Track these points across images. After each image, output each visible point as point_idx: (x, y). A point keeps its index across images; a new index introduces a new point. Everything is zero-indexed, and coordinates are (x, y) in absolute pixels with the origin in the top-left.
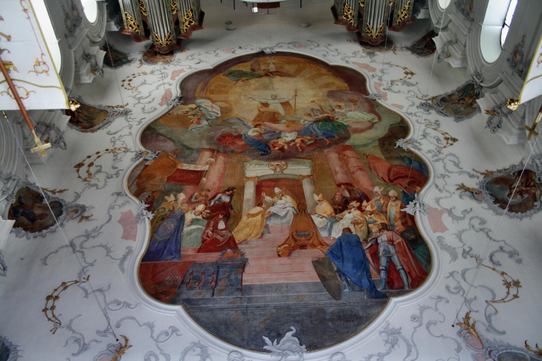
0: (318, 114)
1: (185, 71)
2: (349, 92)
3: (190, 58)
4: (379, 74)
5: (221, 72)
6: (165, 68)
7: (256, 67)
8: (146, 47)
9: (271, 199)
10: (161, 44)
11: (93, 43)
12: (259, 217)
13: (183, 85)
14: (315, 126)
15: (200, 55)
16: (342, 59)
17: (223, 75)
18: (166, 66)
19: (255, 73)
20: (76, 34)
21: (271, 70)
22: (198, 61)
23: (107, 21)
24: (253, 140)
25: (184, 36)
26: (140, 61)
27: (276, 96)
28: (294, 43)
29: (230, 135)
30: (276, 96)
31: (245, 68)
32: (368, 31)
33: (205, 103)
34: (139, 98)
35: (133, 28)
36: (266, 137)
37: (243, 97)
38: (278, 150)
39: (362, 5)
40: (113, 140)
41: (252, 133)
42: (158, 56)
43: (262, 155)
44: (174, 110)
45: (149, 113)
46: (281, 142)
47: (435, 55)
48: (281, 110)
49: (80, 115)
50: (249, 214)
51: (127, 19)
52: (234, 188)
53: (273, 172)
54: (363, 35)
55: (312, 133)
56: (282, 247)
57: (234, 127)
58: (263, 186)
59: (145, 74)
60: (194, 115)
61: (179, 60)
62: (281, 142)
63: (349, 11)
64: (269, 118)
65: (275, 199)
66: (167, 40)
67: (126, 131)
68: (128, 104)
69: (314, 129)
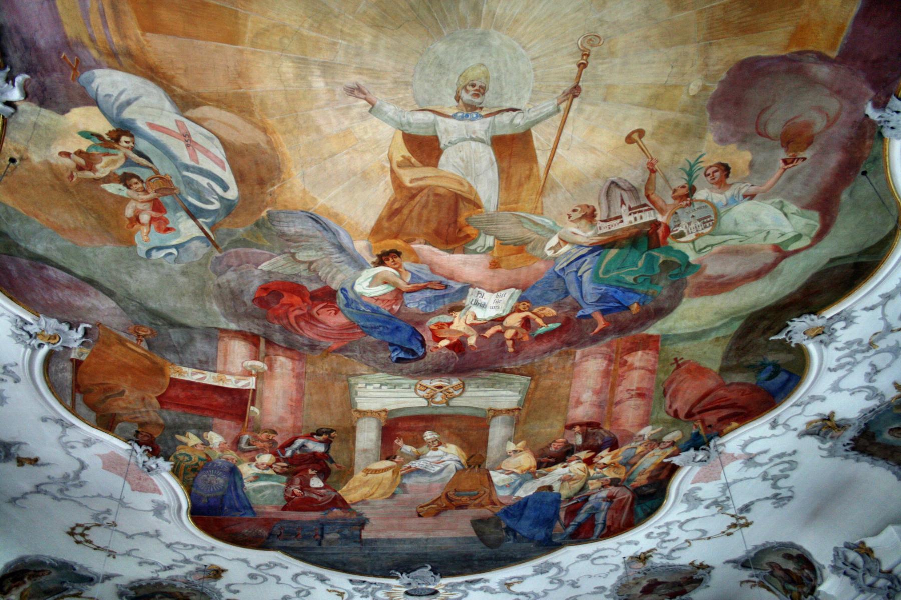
0: (624, 211)
9: (415, 450)
12: (389, 474)
24: (375, 311)
29: (296, 289)
36: (414, 304)
37: (319, 84)
38: (448, 347)
43: (399, 360)
46: (459, 323)
50: (368, 470)
52: (332, 431)
53: (424, 403)
55: (567, 293)
56: (426, 508)
57: (302, 256)
58: (396, 430)
60: (125, 180)
62: (459, 323)
64: (433, 225)
65: (424, 449)
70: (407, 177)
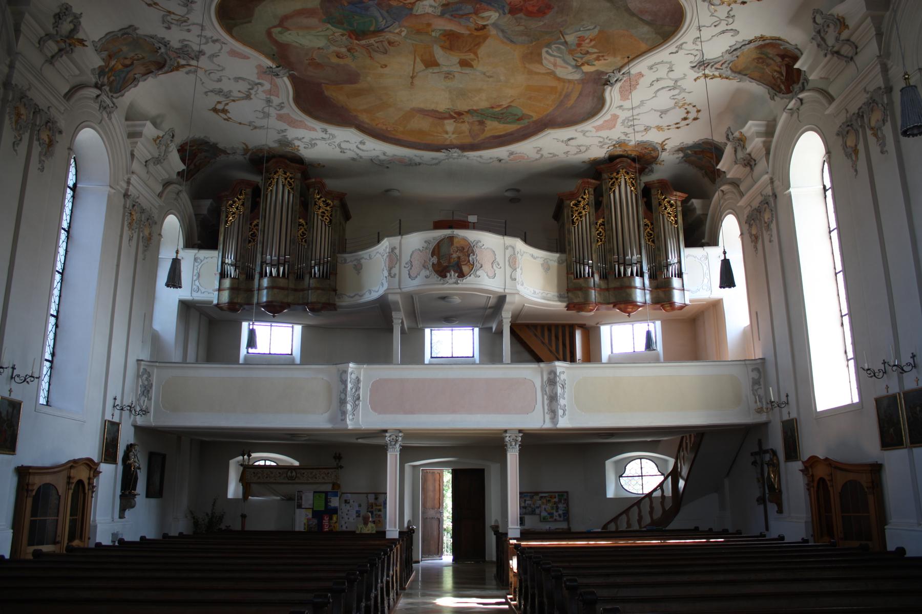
0: (376, 45)
1: (594, 127)
3: (583, 149)
4: (273, 112)
5: (535, 122)
6: (626, 134)
7: (476, 128)
8: (652, 171)
10: (628, 173)
11: (735, 183)
13: (600, 104)
14: (383, 24)
16: (334, 136)
17: (530, 117)
18: (623, 137)
19: (479, 119)
20: (760, 199)
21: (452, 121)
22: (571, 142)
26: (664, 150)
27: (446, 77)
29: (530, 14)
31: (494, 127)
33: (567, 72)
34: (674, 88)
35: (669, 202)
36: (468, 8)
37: (502, 78)
40: (730, 20)
41: (492, 16)
44: (620, 64)
45: (662, 62)
47: (179, 140)
48: (439, 54)
49: (777, 69)
51: (676, 216)
54: (299, 175)
55: (387, 12)
57: (522, 28)
59: (659, 128)
60: (588, 53)
61: (601, 147)
63: (323, 212)
66: (617, 179)
67: (706, 33)
68: (695, 80)
69: (384, 18)
70: (472, 56)
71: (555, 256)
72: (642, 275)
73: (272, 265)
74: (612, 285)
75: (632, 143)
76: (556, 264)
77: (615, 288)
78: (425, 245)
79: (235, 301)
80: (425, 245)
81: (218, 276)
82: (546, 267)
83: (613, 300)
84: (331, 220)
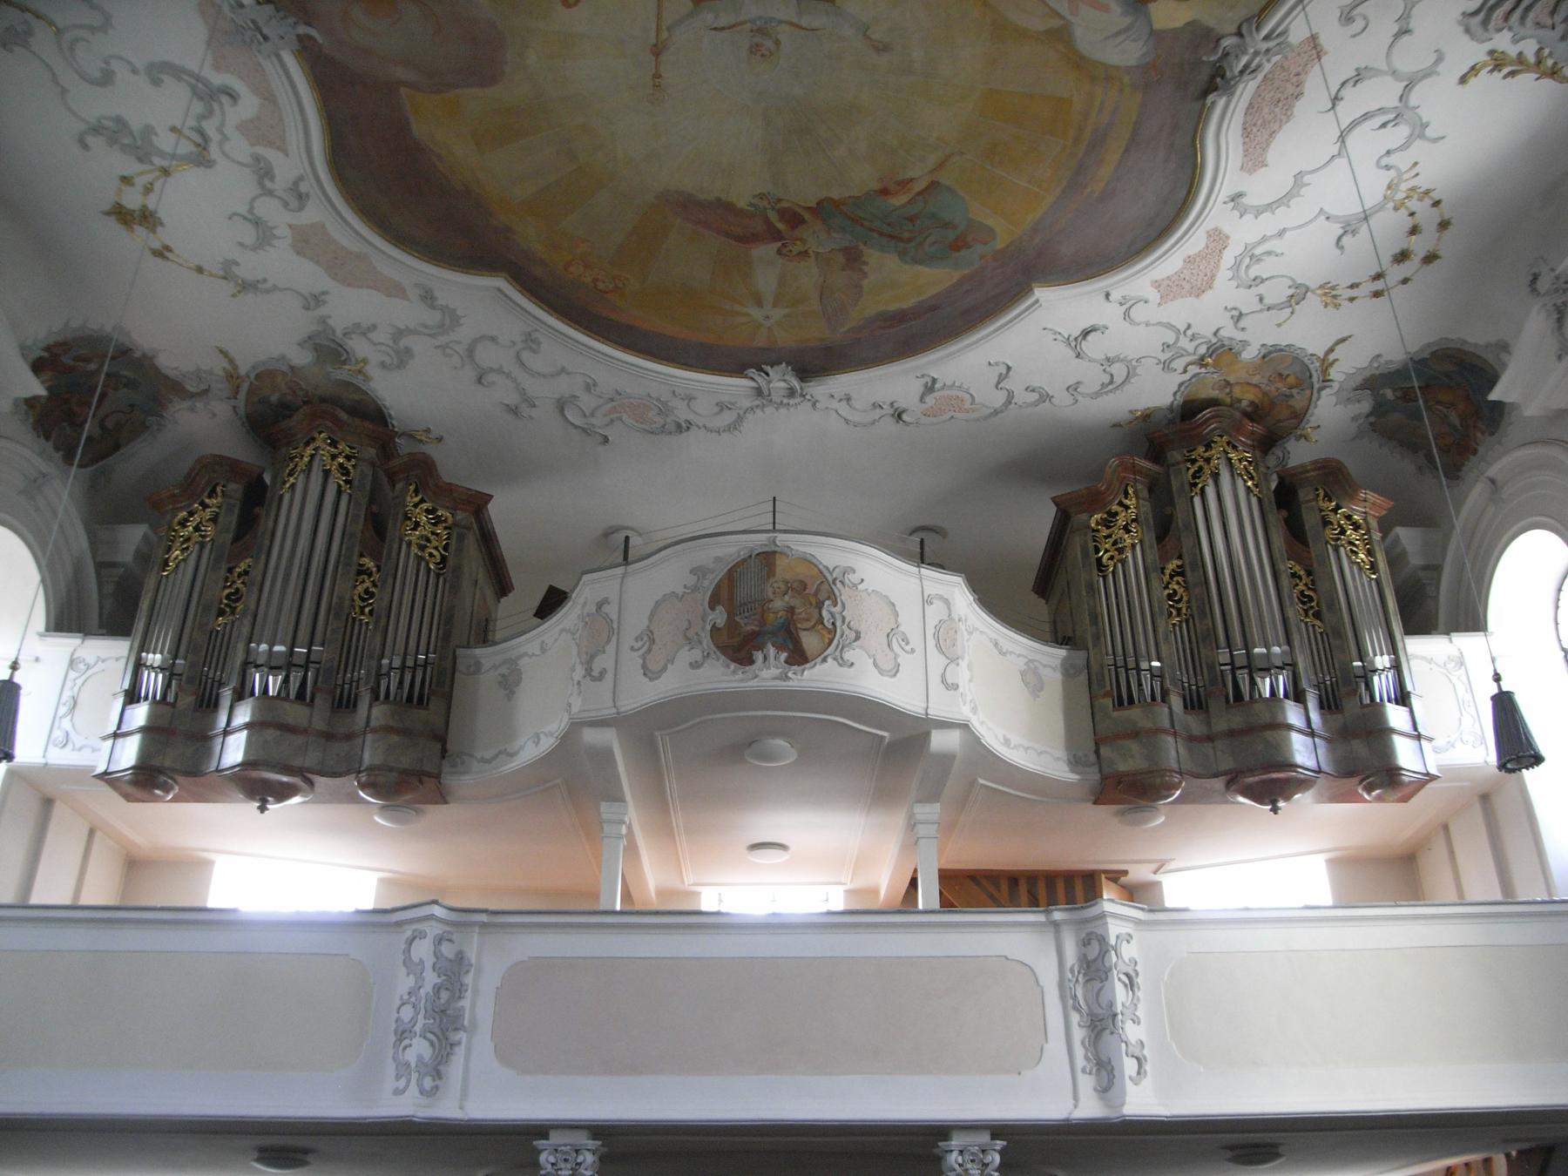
1: (1157, 284)
2: (401, 73)
3: (1119, 371)
15: (1073, 388)
18: (1229, 332)
22: (1088, 346)
23: (1436, 569)
25: (1135, 470)
28: (663, 430)
30: (755, 49)
32: (349, 465)
35: (1349, 518)
39: (369, 563)
42: (1248, 397)
51: (1370, 553)
54: (373, 451)
59: (1330, 294)
66: (1208, 460)
68: (1463, 80)
71: (1056, 655)
72: (1299, 697)
73: (274, 669)
74: (1221, 724)
75: (1249, 354)
76: (1058, 676)
77: (1231, 734)
78: (691, 580)
79: (156, 762)
80: (691, 580)
81: (121, 700)
82: (1032, 680)
83: (1227, 763)
84: (443, 557)
